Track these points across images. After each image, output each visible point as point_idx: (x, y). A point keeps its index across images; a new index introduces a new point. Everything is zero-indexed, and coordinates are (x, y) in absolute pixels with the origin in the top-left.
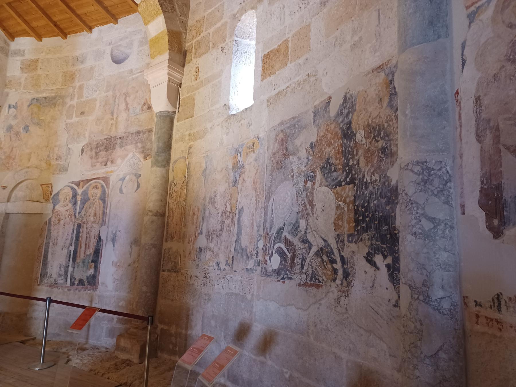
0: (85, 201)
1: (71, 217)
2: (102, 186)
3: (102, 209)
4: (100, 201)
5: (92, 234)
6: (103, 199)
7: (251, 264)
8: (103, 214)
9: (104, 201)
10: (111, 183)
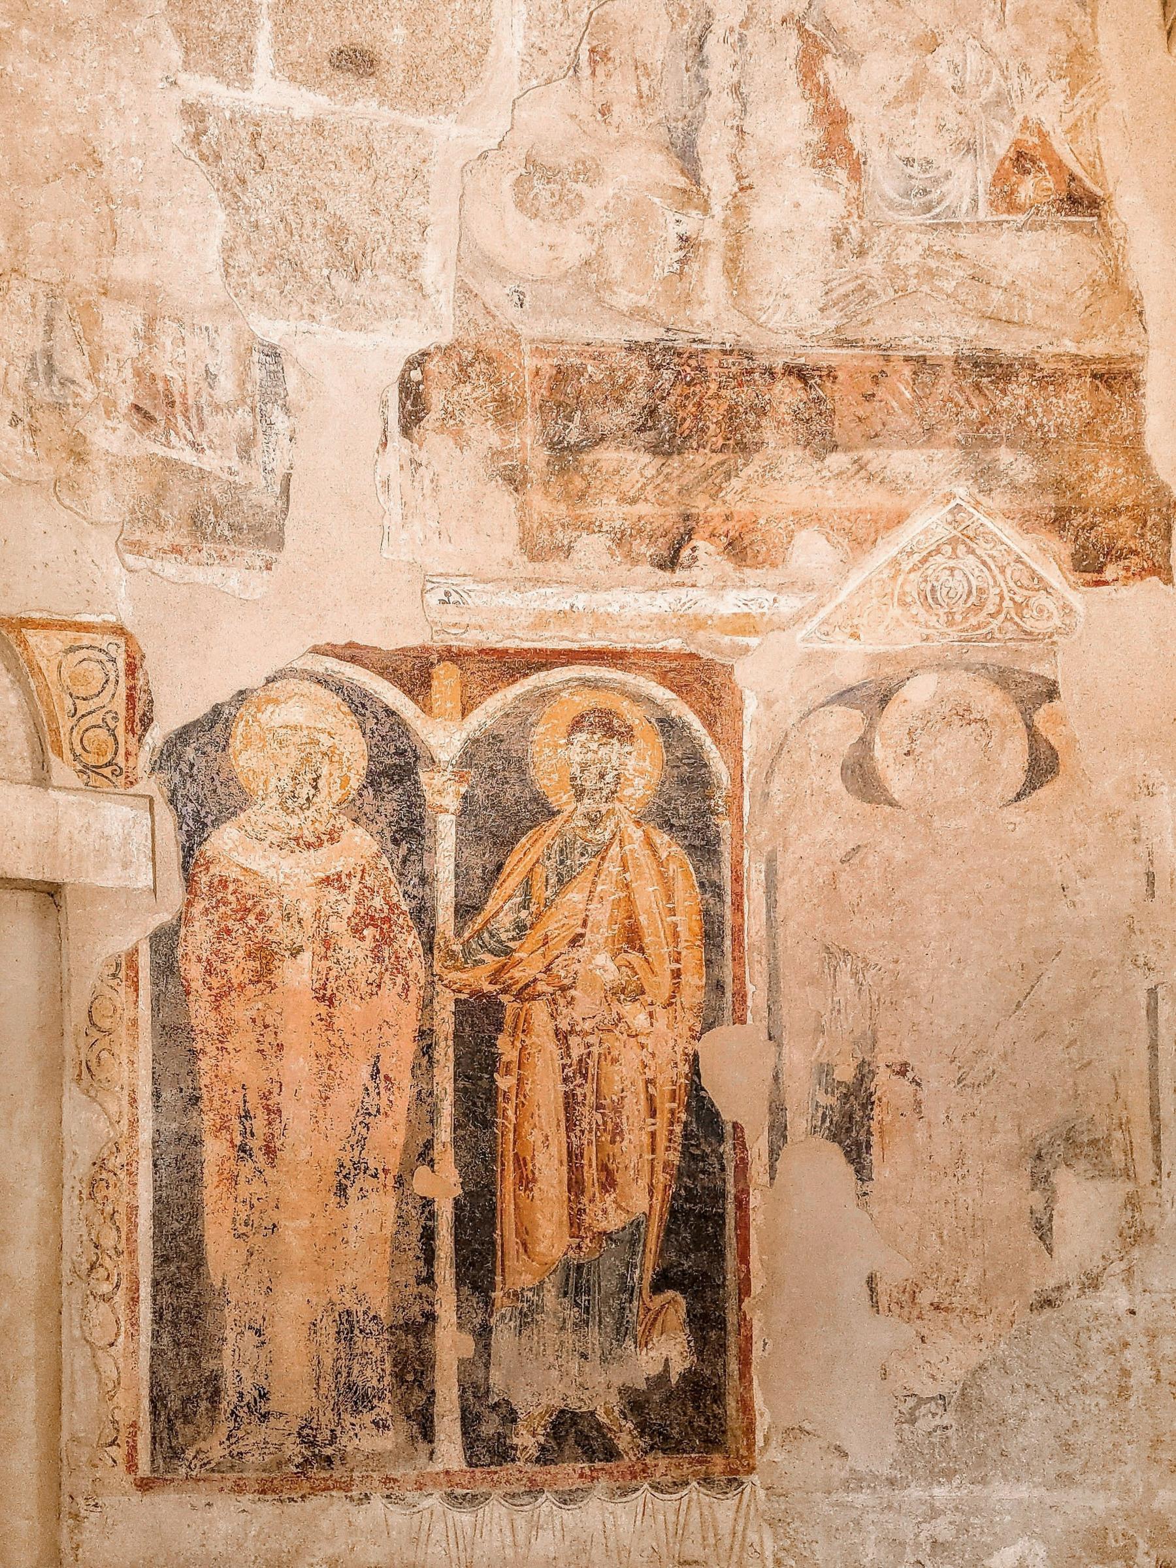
0: (506, 817)
1: (386, 939)
2: (667, 725)
3: (688, 898)
4: (662, 839)
5: (624, 1075)
6: (691, 812)
10: (751, 707)
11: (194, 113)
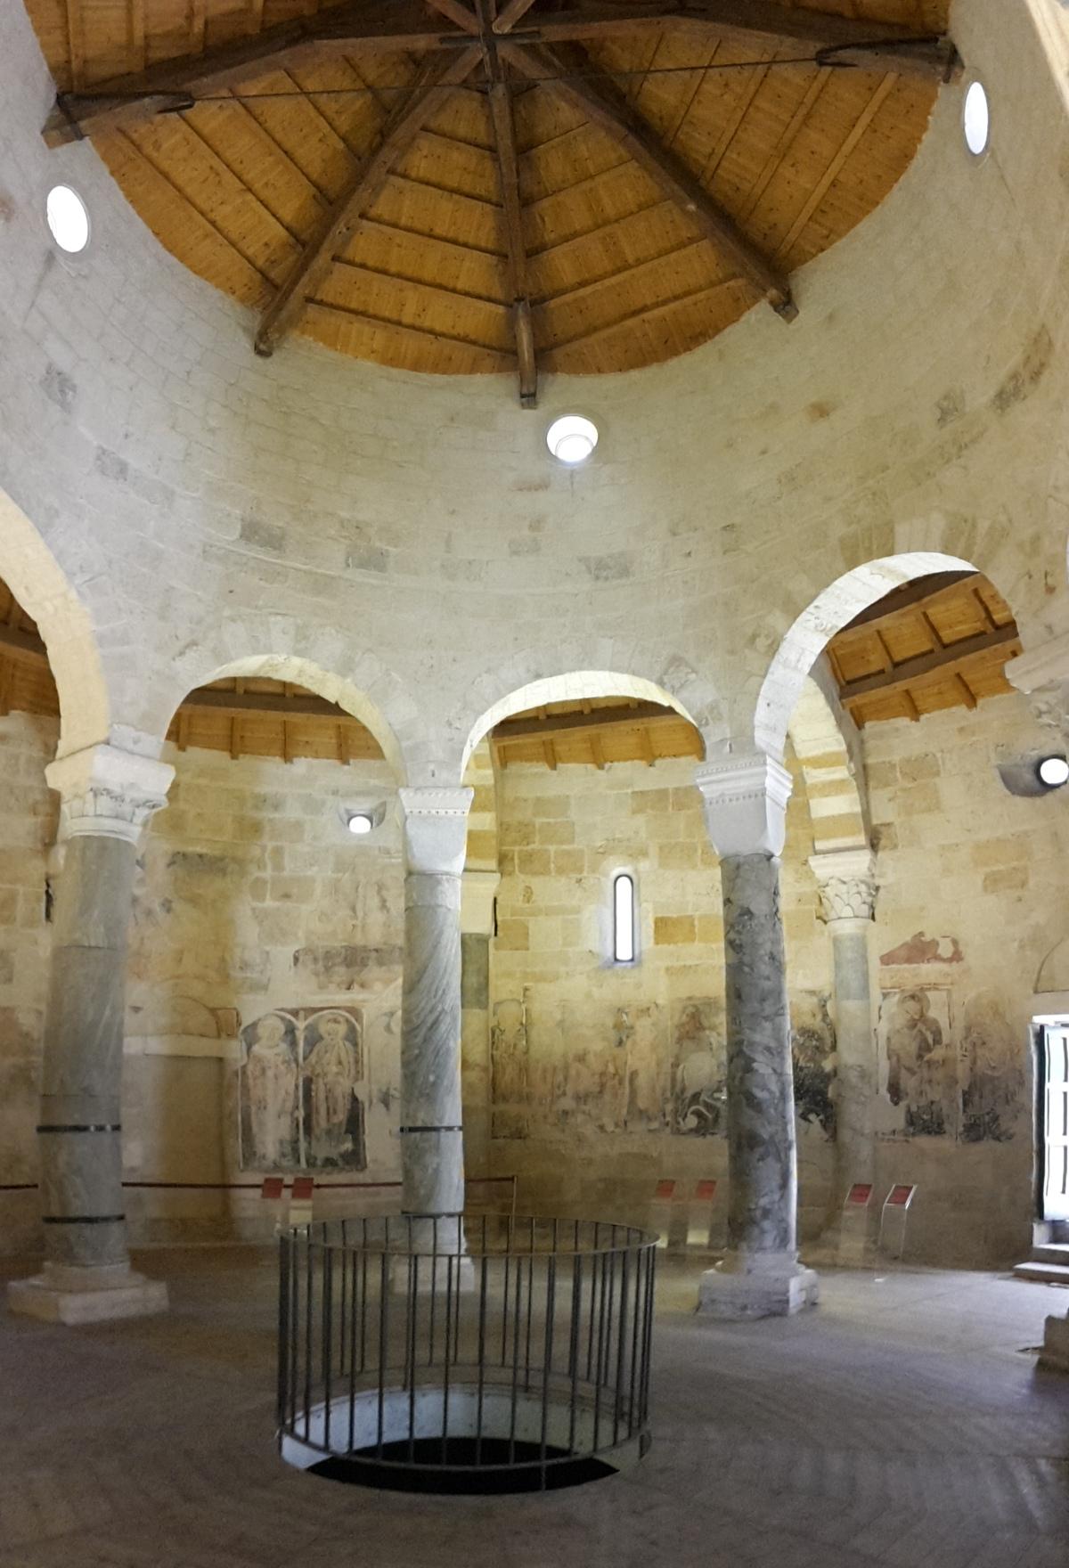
2: (347, 1021)
3: (351, 1054)
5: (338, 1091)
6: (352, 1037)
7: (655, 1125)
8: (357, 1062)
9: (355, 1045)
11: (254, 909)
